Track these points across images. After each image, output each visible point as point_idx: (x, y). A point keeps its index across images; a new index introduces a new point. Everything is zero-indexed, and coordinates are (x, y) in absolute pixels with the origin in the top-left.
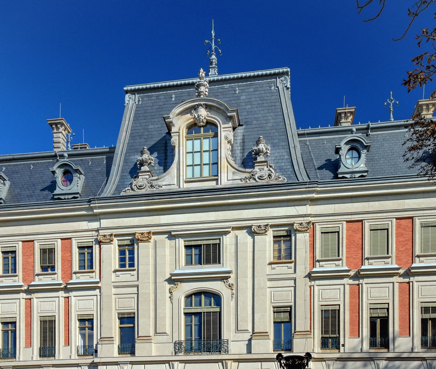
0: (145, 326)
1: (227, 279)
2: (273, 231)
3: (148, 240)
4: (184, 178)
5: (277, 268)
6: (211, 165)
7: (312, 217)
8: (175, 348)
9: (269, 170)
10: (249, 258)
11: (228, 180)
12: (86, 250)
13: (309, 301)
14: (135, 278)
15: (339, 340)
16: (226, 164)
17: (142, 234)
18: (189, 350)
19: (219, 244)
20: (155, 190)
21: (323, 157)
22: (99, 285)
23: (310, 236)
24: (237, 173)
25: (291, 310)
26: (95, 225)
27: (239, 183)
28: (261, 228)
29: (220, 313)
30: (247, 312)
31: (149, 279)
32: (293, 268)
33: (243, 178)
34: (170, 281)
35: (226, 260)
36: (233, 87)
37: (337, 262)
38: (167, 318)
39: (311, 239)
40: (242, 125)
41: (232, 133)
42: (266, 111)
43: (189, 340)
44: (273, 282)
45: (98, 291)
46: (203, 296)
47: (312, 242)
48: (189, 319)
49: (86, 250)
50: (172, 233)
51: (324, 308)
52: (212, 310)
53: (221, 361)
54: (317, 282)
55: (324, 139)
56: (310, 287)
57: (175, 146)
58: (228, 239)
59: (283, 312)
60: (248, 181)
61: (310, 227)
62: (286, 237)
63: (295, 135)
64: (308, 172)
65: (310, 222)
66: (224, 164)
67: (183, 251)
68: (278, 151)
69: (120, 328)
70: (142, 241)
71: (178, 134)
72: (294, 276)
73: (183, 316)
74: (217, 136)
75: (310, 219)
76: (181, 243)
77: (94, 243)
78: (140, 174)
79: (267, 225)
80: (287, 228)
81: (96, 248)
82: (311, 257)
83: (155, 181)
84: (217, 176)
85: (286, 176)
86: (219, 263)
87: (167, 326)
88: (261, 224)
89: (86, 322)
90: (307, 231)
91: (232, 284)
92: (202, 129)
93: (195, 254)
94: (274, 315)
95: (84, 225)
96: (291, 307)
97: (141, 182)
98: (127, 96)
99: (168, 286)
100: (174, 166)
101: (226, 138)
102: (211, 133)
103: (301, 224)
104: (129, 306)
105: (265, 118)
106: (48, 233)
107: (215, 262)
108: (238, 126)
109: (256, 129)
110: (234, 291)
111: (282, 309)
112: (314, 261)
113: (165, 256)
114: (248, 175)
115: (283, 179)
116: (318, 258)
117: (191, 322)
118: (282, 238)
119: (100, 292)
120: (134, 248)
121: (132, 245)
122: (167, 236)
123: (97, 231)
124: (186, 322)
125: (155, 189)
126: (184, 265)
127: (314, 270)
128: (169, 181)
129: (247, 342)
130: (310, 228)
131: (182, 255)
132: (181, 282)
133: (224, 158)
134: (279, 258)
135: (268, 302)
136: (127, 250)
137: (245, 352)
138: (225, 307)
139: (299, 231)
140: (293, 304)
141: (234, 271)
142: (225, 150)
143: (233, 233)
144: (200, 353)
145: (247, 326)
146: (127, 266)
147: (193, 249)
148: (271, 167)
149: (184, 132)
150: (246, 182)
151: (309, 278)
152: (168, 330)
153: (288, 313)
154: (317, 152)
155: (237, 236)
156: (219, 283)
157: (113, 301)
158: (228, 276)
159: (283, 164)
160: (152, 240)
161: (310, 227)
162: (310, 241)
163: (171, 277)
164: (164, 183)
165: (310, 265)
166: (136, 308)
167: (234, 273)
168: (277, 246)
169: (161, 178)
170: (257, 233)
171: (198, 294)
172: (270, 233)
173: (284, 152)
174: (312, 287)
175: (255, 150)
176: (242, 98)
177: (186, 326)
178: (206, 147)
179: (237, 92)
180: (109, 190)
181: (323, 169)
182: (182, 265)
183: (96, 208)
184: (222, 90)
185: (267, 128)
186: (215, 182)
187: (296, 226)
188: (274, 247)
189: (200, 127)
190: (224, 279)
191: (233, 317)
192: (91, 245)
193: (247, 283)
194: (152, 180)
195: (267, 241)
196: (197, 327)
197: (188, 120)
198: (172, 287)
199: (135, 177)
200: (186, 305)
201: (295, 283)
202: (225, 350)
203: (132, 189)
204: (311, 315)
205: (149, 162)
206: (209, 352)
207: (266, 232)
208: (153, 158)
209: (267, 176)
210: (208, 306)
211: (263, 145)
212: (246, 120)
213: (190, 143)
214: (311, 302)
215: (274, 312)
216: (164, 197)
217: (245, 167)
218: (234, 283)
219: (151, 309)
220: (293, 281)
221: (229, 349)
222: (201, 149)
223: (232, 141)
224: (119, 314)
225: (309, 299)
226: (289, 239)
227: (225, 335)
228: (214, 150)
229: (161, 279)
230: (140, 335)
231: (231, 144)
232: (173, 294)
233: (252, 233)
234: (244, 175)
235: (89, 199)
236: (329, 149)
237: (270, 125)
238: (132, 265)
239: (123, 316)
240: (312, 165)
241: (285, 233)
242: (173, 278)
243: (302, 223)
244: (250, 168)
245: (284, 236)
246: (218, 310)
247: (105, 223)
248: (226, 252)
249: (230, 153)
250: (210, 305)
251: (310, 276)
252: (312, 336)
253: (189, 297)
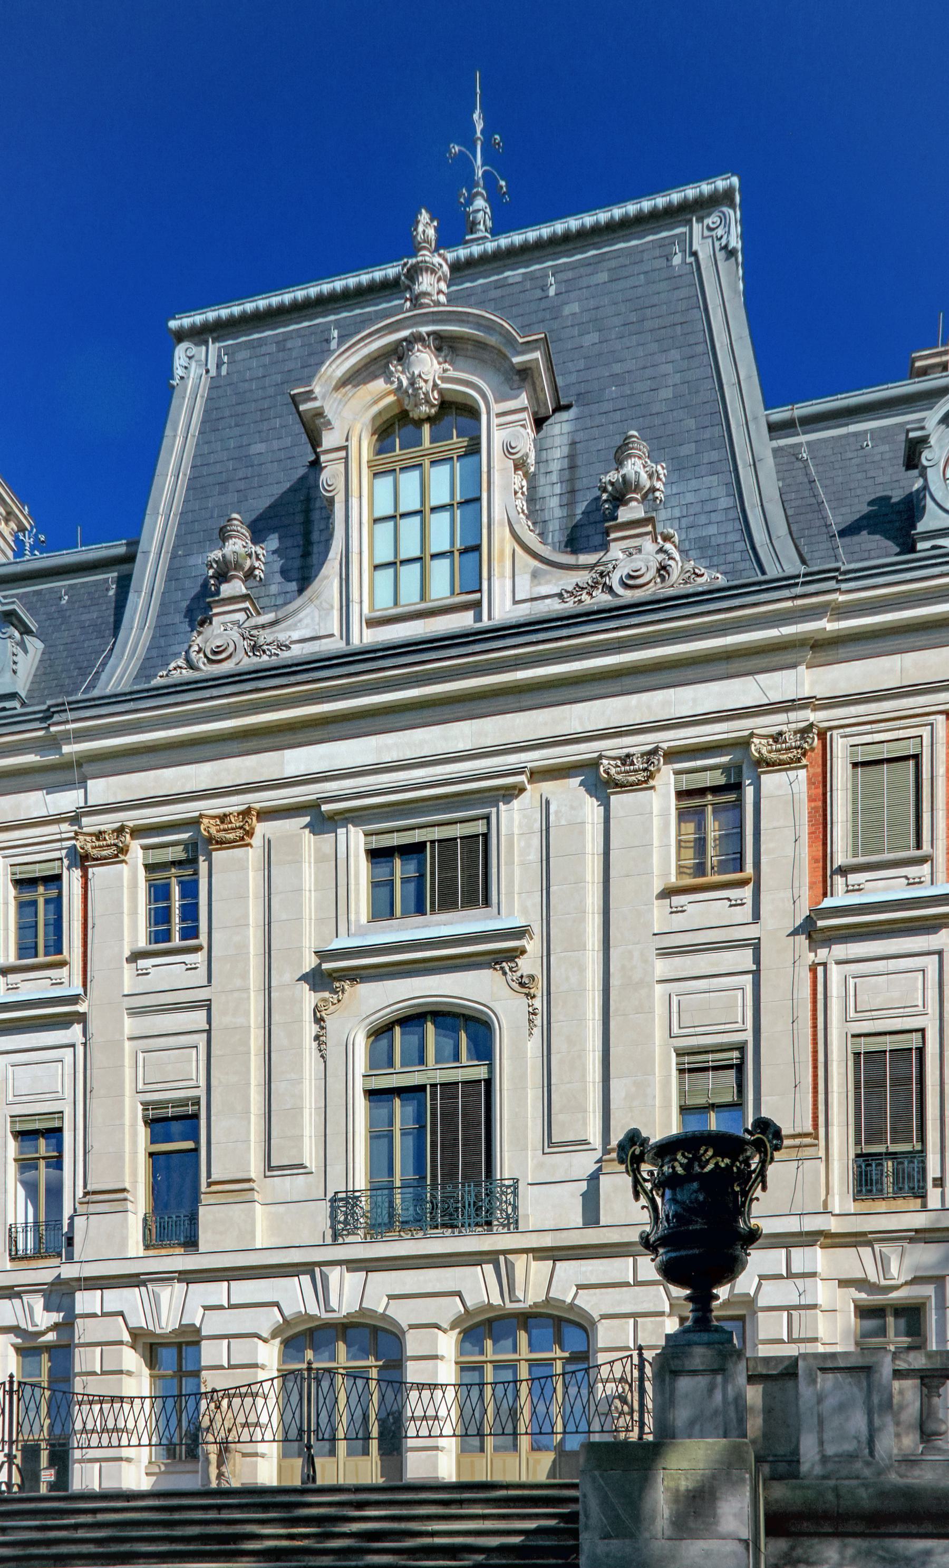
0: (232, 1146)
1: (512, 959)
2: (677, 773)
3: (242, 839)
4: (366, 610)
5: (689, 908)
6: (457, 554)
7: (816, 708)
8: (333, 1217)
9: (661, 550)
10: (589, 878)
11: (515, 602)
12: (41, 889)
13: (810, 1023)
14: (200, 976)
15: (923, 1162)
16: (509, 543)
17: (223, 818)
18: (382, 1226)
19: (486, 836)
20: (264, 660)
21: (859, 492)
22: (81, 1008)
23: (810, 782)
24: (546, 572)
25: (743, 1059)
27: (554, 607)
28: (632, 764)
30: (584, 1076)
31: (245, 976)
32: (749, 902)
33: (570, 589)
34: (318, 979)
35: (510, 893)
36: (538, 274)
37: (912, 871)
38: (306, 1113)
39: (813, 791)
40: (568, 407)
41: (529, 432)
42: (654, 347)
43: (381, 1187)
44: (678, 961)
45: (77, 1028)
46: (430, 1028)
47: (820, 804)
48: (384, 1112)
50: (324, 808)
51: (865, 1045)
52: (460, 1075)
53: (491, 1257)
54: (840, 950)
55: (865, 432)
56: (813, 969)
57: (331, 501)
58: (516, 816)
59: (715, 1068)
60: (585, 597)
61: (810, 749)
63: (755, 418)
64: (805, 550)
65: (812, 725)
66: (500, 543)
67: (361, 868)
68: (694, 484)
69: (151, 1155)
70: (223, 844)
71: (343, 454)
72: (751, 932)
73: (361, 1103)
74: (478, 451)
75: (812, 716)
76: (355, 840)
77: (66, 862)
78: (215, 611)
79: (654, 752)
80: (725, 759)
81: (72, 880)
82: (814, 860)
83: (268, 631)
84: (480, 591)
85: (722, 568)
86: (487, 902)
87: (306, 1140)
88: (632, 750)
90: (799, 760)
91: (532, 977)
92: (426, 428)
93: (404, 881)
94: (681, 1084)
95: (35, 803)
96: (741, 1048)
97: (220, 635)
98: (181, 352)
99: (309, 998)
100: (331, 570)
101: (509, 450)
102: (458, 442)
103: (777, 737)
104: (180, 1075)
105: (649, 372)
108: (554, 411)
109: (617, 416)
110: (537, 1003)
111: (710, 1057)
112: (826, 872)
113: (300, 890)
114: (584, 577)
115: (710, 578)
116: (841, 858)
117: (391, 1123)
118: (710, 797)
119: (85, 1035)
120: (196, 873)
121: (192, 862)
122: (308, 819)
123: (75, 819)
124: (372, 1121)
125: (265, 658)
126: (364, 919)
127: (828, 903)
128: (315, 623)
129: (584, 1186)
130: (812, 749)
131: (357, 884)
132: (354, 980)
133: (501, 524)
134: (700, 869)
135: (659, 1033)
136: (174, 881)
137: (579, 1222)
138: (505, 1062)
139: (768, 765)
140: (748, 1036)
141: (536, 929)
142: (504, 494)
143: (533, 793)
144: (420, 1234)
145: (585, 1124)
146: (176, 935)
147: (398, 862)
148: (667, 538)
149: (363, 447)
150: (580, 601)
151: (809, 937)
152: (310, 1156)
153: (732, 1073)
154: (840, 479)
155: (548, 802)
156: (486, 974)
157: (128, 1061)
158: (514, 949)
159: (713, 530)
160: (256, 841)
161: (810, 749)
162: (811, 799)
163: (320, 965)
164: (296, 636)
165: (810, 888)
166: (202, 1082)
167: (537, 937)
168: (690, 827)
169: (286, 618)
170: (617, 785)
171: (412, 1020)
172: (667, 780)
173: (714, 486)
174: (820, 969)
175: (612, 484)
176: (567, 310)
177: (371, 1138)
178: (440, 494)
179: (552, 292)
180: (119, 674)
181: (859, 533)
182: (357, 920)
183: (68, 737)
184: (499, 293)
185: (655, 408)
186: (469, 616)
187: (759, 747)
188: (679, 833)
189: (419, 423)
191: (533, 1096)
192: (56, 872)
193: (582, 969)
194: (256, 627)
196: (410, 1140)
197: (375, 402)
198: (324, 1000)
199: (202, 624)
200: (373, 1063)
201: (757, 960)
202: (508, 1217)
203: (191, 666)
204: (815, 1076)
205: (247, 568)
206: (453, 1226)
207: (651, 776)
208: (260, 551)
209: (652, 572)
210: (448, 1062)
211: (639, 462)
212: (583, 388)
213: (384, 485)
214: (815, 1027)
215: (681, 1071)
216: (293, 679)
217: (575, 552)
218: (537, 972)
219: (253, 1082)
220: (749, 952)
221: (521, 1211)
222: (423, 502)
223: (532, 460)
224: (146, 1105)
225: (809, 1014)
226: (732, 797)
227: (507, 1164)
228: (467, 502)
229: (284, 976)
230: (215, 1177)
231: (526, 475)
232: (328, 1024)
233: (602, 787)
234: (570, 580)
235: (44, 707)
236: (884, 464)
237: (666, 393)
238: (190, 932)
239: (161, 1113)
240: (818, 523)
241: (718, 778)
242: (325, 966)
243: (780, 734)
244: (595, 549)
245: (716, 790)
246: (481, 1073)
247: (102, 789)
248: (511, 863)
249: (522, 503)
250: (457, 1058)
251: (812, 931)
252: (822, 1153)
253: (380, 1032)
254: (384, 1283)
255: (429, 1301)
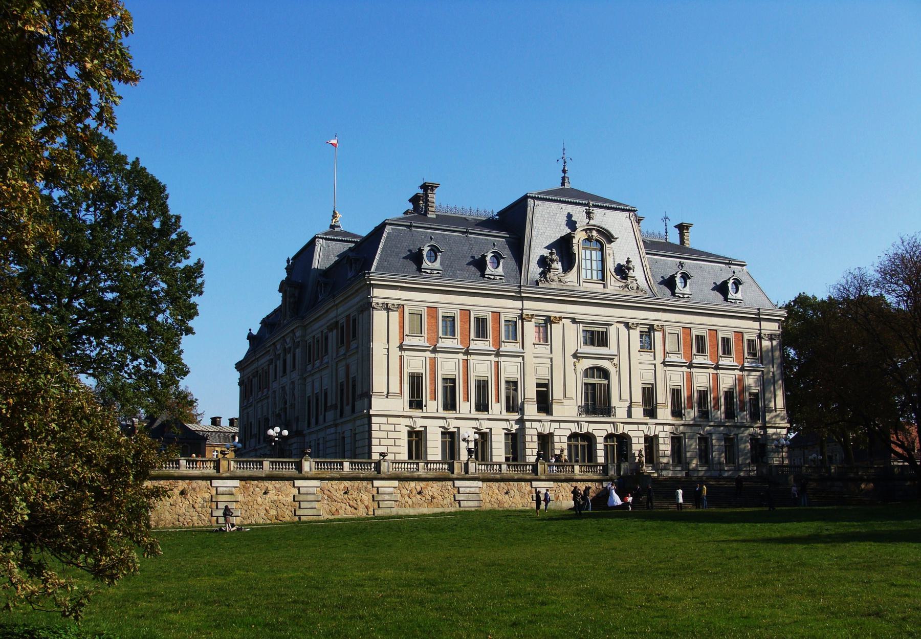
26: (518, 304)
29: (609, 385)
34: (575, 356)
49: (512, 324)
62: (649, 332)
81: (519, 323)
89: (513, 385)
106: (482, 306)
107: (603, 346)
112: (665, 353)
120: (546, 327)
123: (522, 310)
161: (662, 329)
171: (592, 368)
187: (655, 327)
190: (611, 359)
195: (635, 334)
247: (528, 304)
251: (664, 363)
254: (592, 426)
255: (600, 429)
